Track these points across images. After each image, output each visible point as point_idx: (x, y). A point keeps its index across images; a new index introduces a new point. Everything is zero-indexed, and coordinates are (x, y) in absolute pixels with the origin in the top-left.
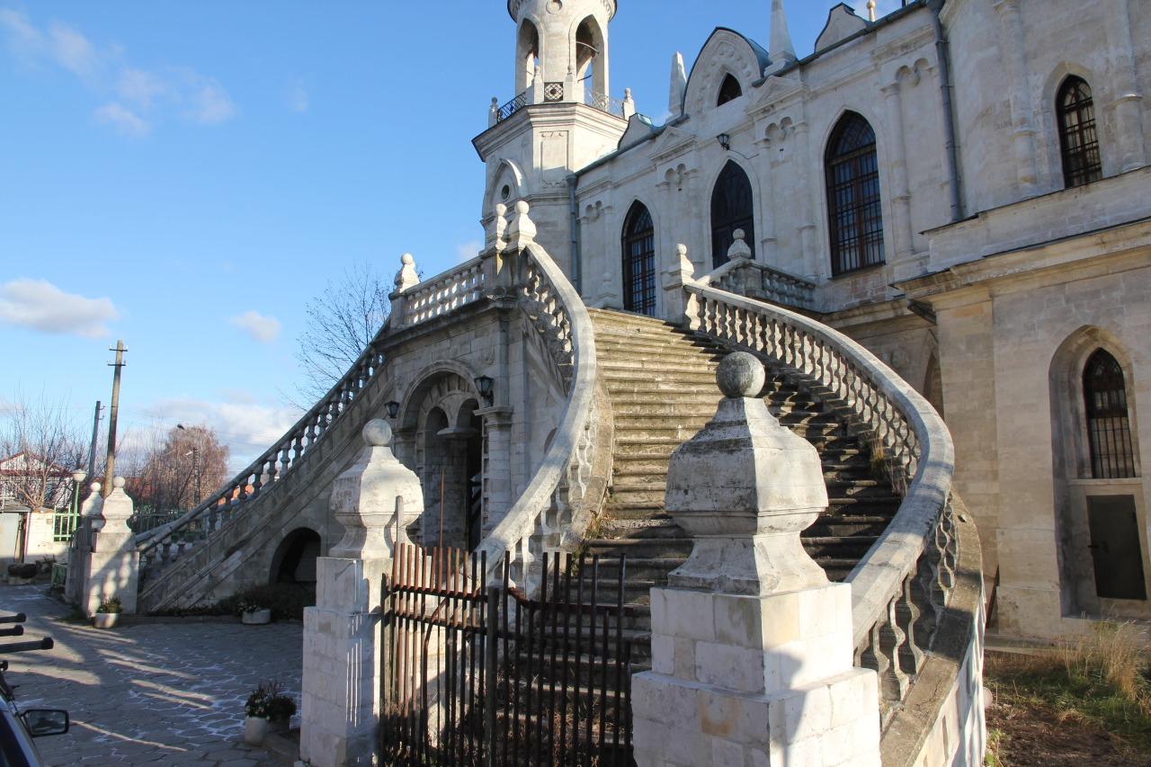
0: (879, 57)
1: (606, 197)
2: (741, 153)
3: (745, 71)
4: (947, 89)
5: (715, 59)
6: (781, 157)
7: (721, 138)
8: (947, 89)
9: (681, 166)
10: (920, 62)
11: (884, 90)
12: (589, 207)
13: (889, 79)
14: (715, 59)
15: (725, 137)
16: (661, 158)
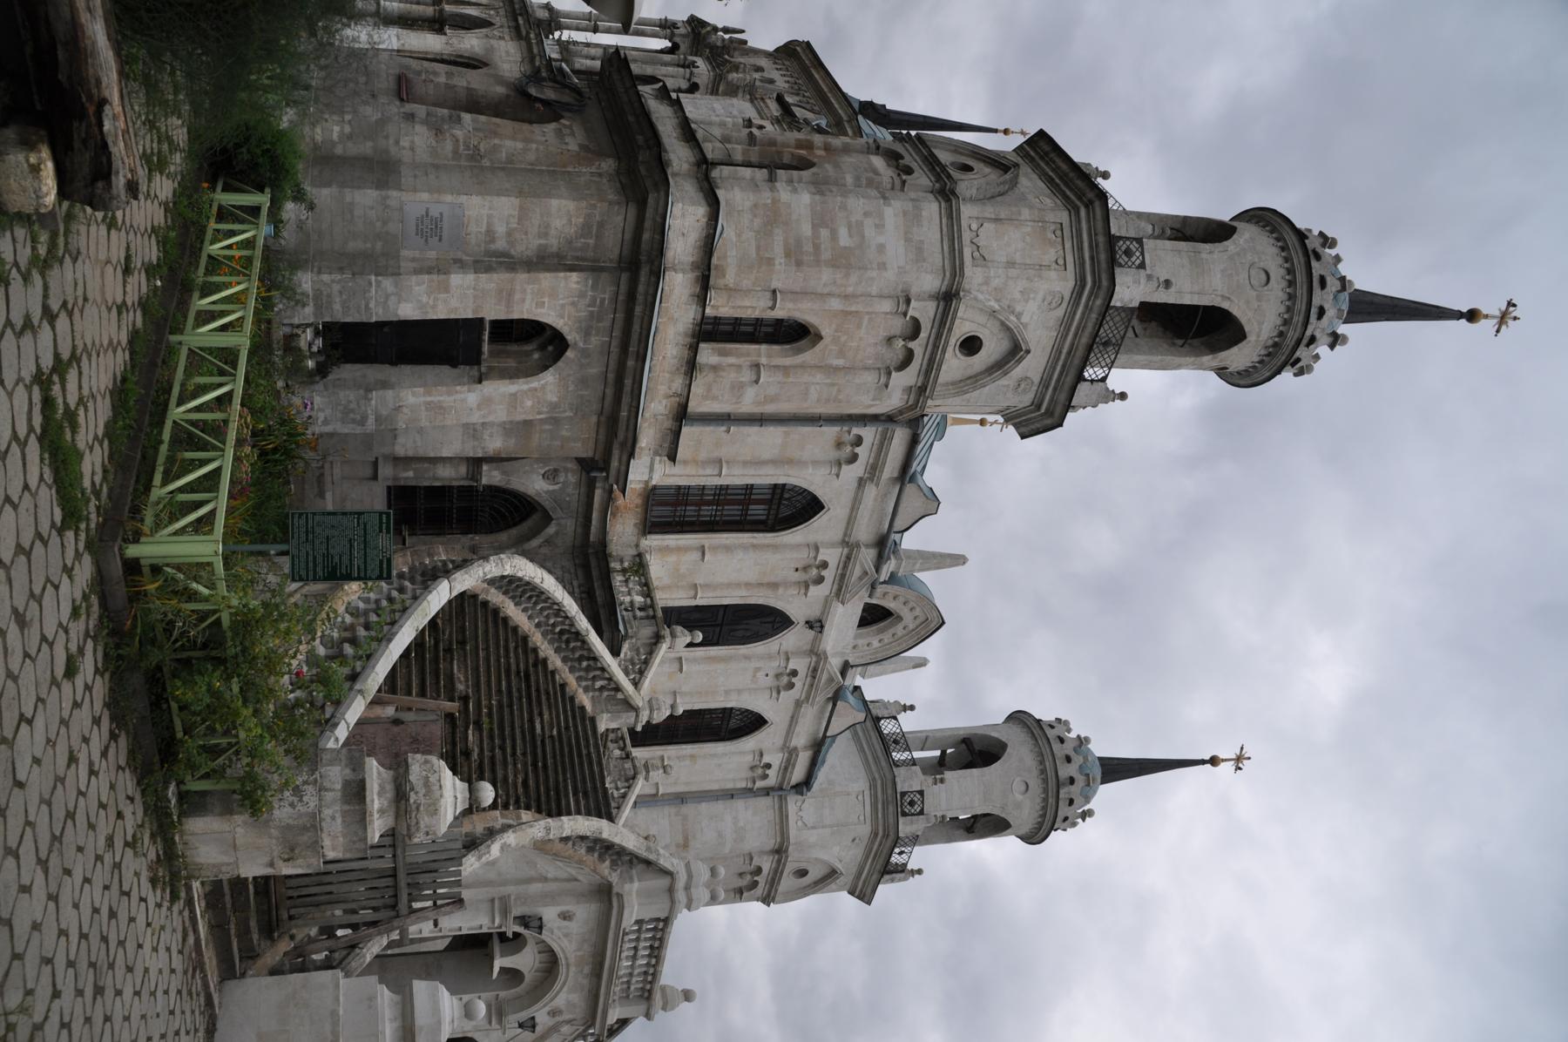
0: (790, 754)
1: (853, 472)
2: (791, 639)
3: (876, 644)
4: (730, 795)
5: (918, 612)
6: (761, 675)
7: (818, 624)
8: (730, 795)
9: (820, 580)
10: (765, 777)
11: (761, 755)
12: (859, 441)
13: (766, 759)
14: (918, 612)
15: (819, 629)
16: (848, 558)
